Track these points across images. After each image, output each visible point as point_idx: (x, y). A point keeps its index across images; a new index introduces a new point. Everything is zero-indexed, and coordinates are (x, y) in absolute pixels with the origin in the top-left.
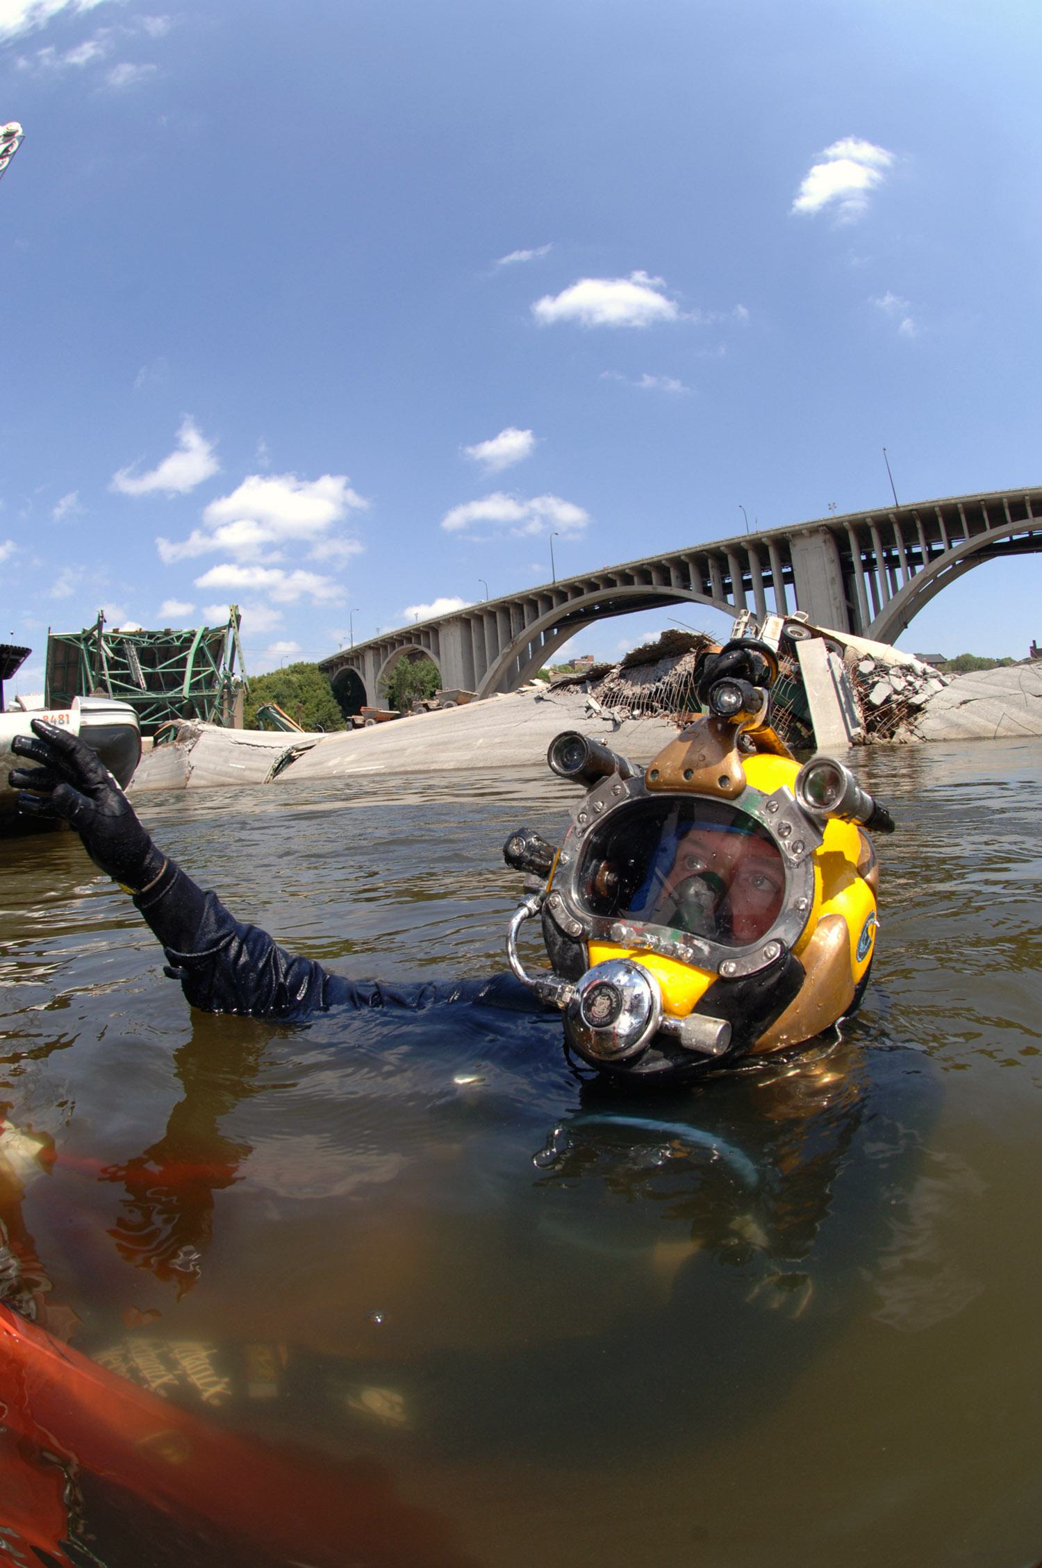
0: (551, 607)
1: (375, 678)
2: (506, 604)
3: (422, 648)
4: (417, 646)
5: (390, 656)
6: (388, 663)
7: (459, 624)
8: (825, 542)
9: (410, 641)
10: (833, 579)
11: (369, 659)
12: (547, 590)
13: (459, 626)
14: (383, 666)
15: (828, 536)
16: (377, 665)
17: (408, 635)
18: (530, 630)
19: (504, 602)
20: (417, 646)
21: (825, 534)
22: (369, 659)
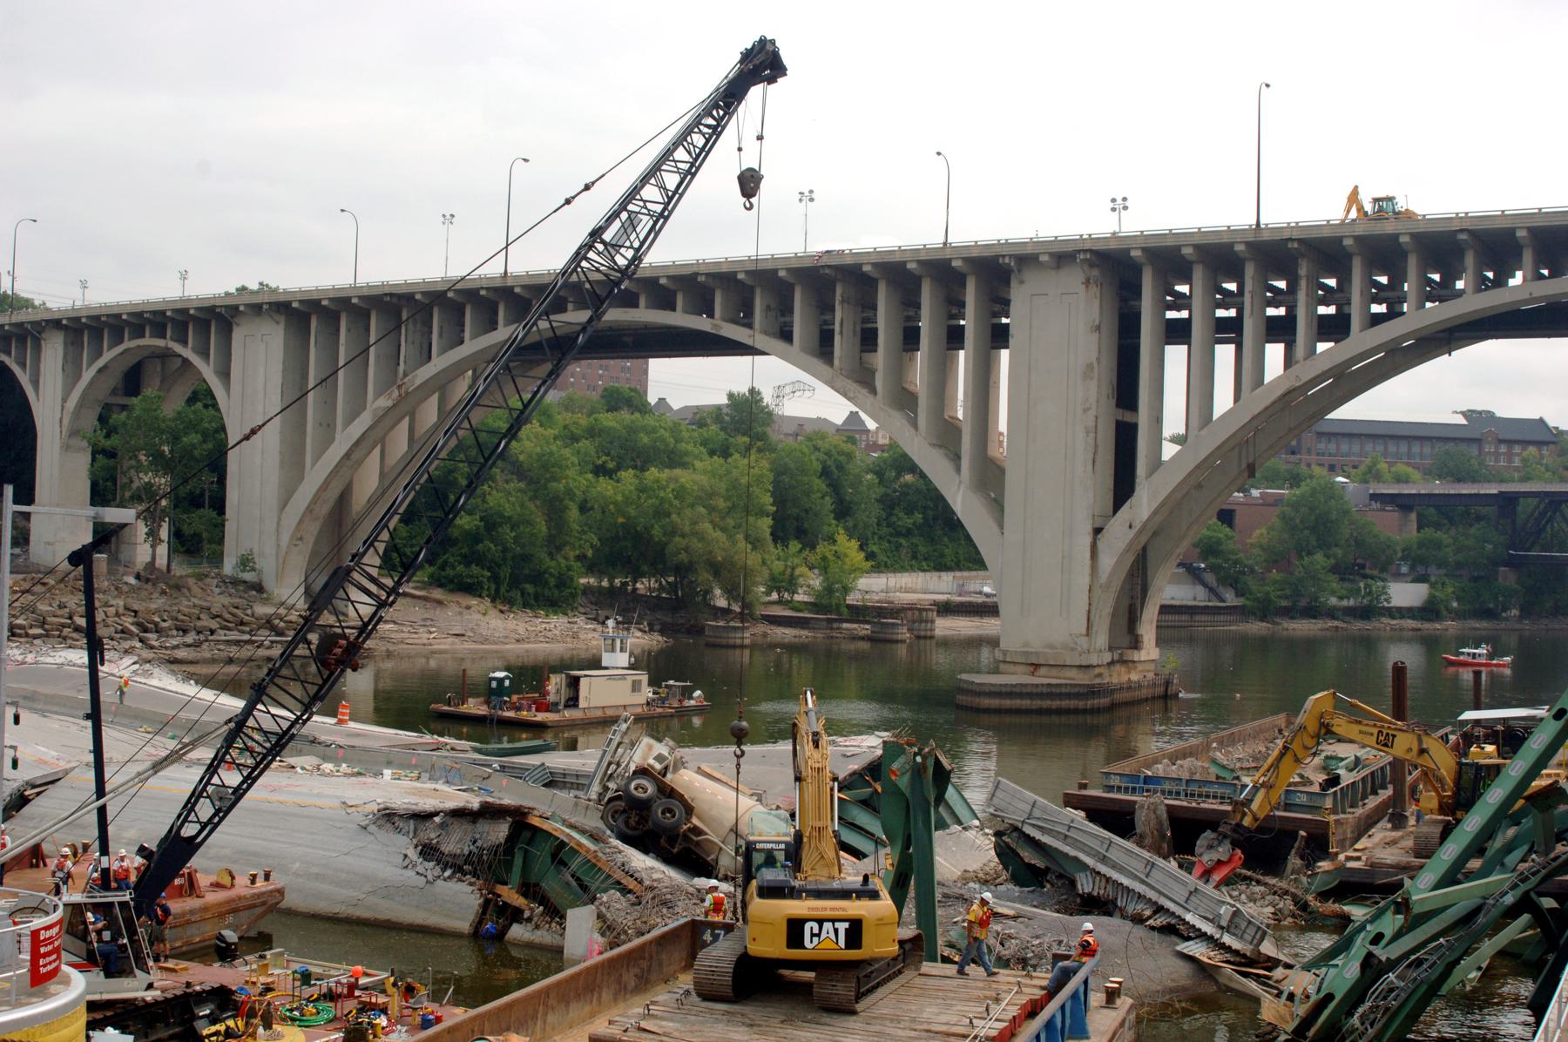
0: (493, 326)
1: (64, 400)
2: (395, 300)
3: (187, 353)
4: (177, 348)
5: (107, 356)
6: (100, 371)
7: (282, 319)
8: (1087, 282)
9: (160, 332)
10: (1090, 366)
11: (53, 351)
12: (487, 289)
13: (282, 325)
14: (88, 375)
15: (1095, 272)
16: (72, 370)
17: (159, 319)
18: (439, 368)
19: (391, 295)
20: (177, 348)
21: (1092, 265)
22: (53, 351)
